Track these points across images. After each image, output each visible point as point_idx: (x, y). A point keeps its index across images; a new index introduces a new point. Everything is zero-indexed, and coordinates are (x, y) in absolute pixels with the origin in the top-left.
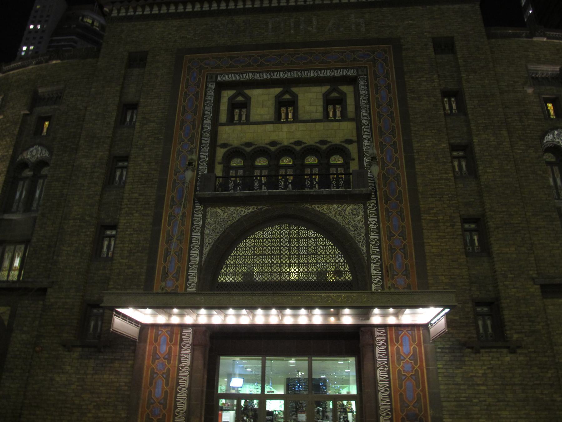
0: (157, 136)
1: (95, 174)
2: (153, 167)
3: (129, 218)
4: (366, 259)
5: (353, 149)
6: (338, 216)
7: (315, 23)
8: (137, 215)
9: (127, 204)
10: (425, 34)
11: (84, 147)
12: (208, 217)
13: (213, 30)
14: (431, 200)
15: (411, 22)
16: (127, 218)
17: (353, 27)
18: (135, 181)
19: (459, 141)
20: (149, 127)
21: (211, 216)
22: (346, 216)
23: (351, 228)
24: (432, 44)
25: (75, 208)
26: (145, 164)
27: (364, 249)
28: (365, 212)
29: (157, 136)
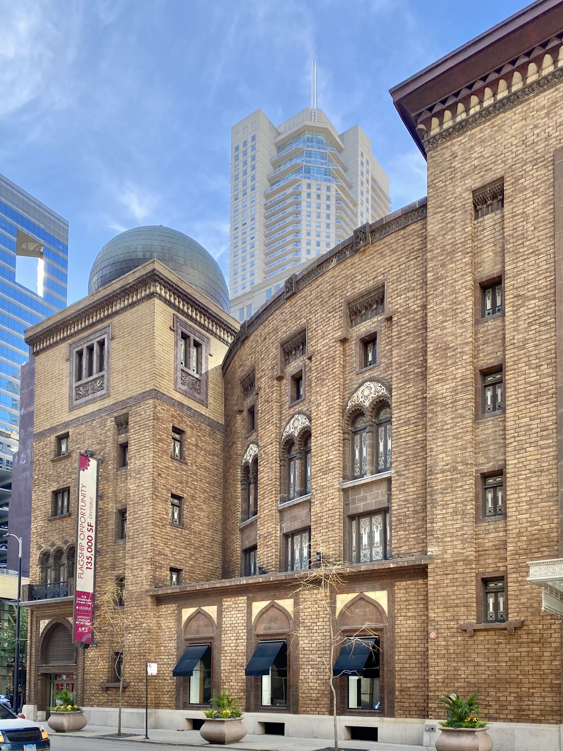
3: (521, 455)
9: (514, 437)
16: (517, 456)
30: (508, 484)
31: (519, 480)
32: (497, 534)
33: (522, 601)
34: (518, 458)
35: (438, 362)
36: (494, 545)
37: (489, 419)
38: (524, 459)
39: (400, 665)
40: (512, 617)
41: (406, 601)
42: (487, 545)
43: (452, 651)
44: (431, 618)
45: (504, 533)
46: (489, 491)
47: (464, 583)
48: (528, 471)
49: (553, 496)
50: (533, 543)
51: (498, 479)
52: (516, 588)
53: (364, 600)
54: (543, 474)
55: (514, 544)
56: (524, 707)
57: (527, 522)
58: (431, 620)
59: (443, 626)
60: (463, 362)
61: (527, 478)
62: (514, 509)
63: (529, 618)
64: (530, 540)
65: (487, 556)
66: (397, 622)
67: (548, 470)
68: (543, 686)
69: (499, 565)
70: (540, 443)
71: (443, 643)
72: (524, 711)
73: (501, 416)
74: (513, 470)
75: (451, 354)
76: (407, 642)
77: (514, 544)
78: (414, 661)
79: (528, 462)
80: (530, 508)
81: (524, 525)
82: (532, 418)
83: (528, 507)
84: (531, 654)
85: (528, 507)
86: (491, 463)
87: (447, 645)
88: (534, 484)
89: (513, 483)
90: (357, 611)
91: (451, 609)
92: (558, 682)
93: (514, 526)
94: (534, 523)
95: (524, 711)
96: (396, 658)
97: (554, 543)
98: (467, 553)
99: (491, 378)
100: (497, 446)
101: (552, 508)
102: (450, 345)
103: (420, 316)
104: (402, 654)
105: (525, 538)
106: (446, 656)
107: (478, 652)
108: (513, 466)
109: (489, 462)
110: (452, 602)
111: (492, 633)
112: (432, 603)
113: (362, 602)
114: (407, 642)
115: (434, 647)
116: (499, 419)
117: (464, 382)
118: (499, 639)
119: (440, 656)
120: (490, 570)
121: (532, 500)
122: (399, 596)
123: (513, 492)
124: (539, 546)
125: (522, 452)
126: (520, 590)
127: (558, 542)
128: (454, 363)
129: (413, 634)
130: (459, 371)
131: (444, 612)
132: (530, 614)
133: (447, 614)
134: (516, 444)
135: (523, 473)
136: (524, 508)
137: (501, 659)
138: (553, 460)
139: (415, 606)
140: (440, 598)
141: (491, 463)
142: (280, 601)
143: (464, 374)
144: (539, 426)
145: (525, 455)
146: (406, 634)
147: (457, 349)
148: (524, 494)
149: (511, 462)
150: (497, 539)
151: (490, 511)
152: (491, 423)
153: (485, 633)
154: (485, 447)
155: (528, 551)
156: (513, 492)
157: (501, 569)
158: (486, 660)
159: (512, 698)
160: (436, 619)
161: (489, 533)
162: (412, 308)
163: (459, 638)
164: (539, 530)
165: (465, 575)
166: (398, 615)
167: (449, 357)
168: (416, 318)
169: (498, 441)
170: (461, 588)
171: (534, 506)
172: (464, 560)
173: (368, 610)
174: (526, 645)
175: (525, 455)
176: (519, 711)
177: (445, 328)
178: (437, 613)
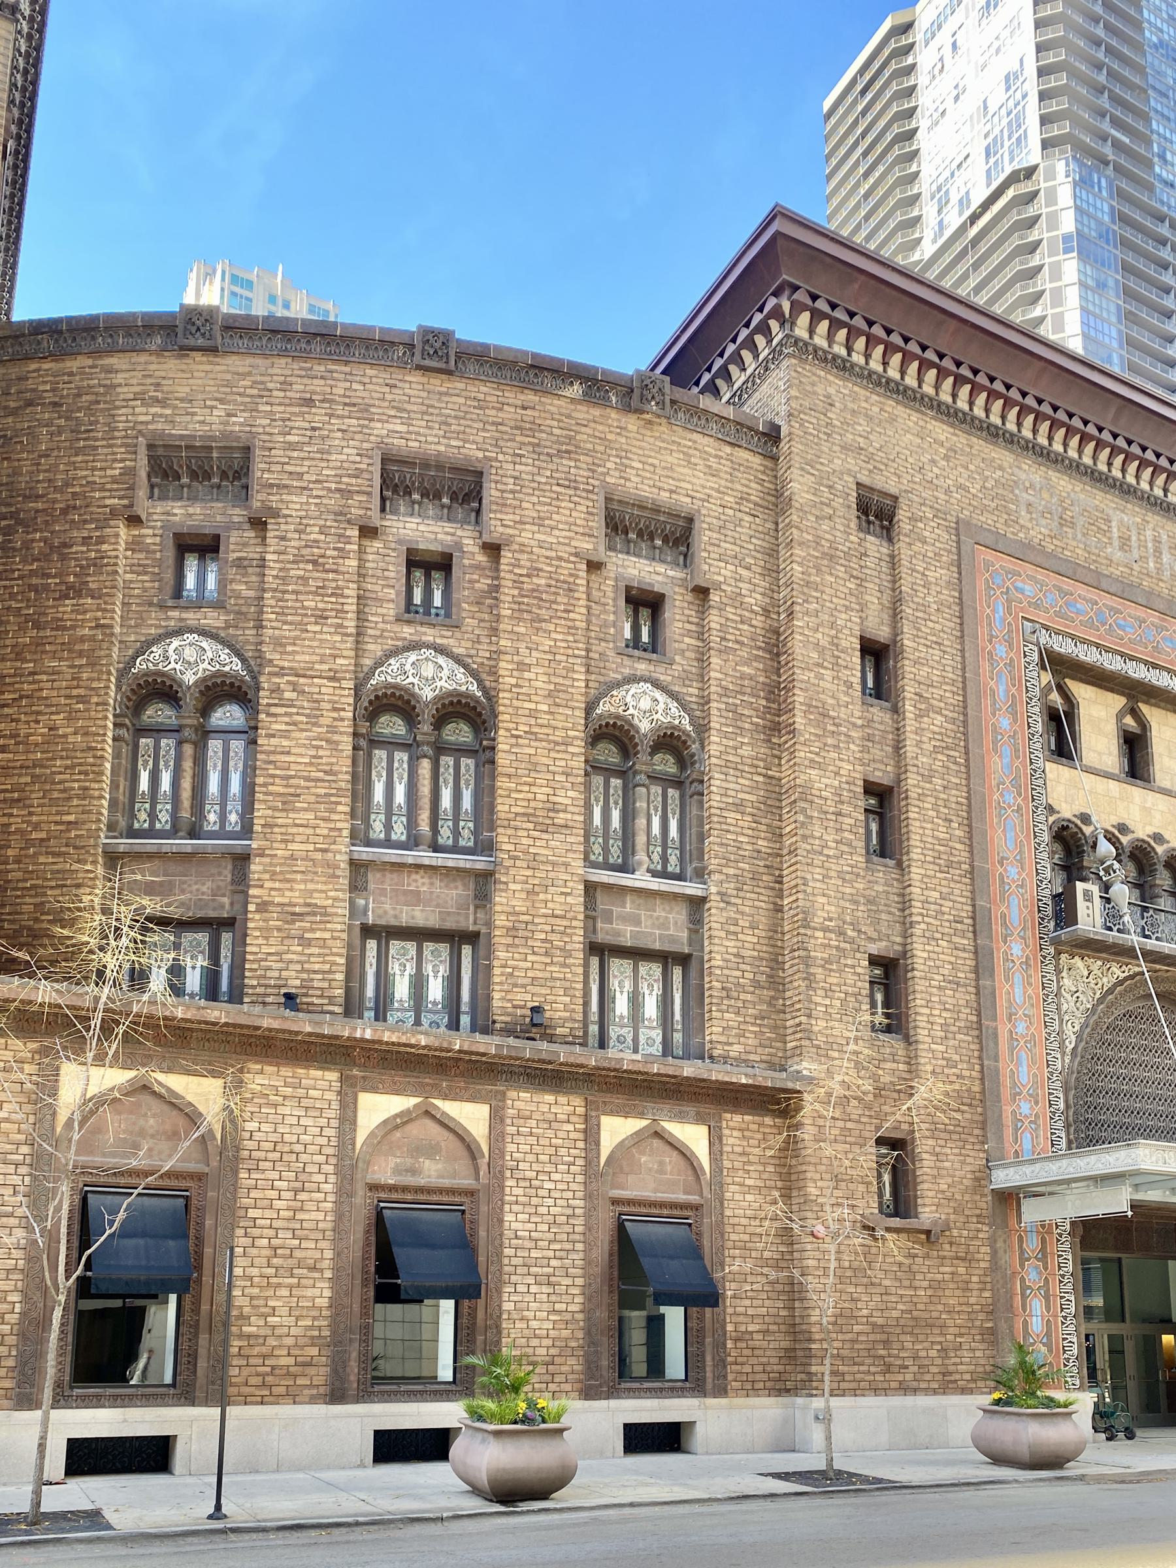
41: (744, 1154)
43: (847, 1264)
53: (662, 1138)
56: (951, 1368)
58: (812, 1201)
66: (728, 1195)
68: (973, 1331)
72: (951, 1373)
90: (643, 1159)
95: (951, 1373)
113: (656, 1143)
114: (746, 1238)
122: (731, 1141)
129: (757, 1222)
133: (837, 1193)
139: (761, 1168)
142: (447, 1103)
146: (744, 1221)
159: (933, 1353)
166: (729, 1180)
173: (667, 1160)
176: (944, 1374)
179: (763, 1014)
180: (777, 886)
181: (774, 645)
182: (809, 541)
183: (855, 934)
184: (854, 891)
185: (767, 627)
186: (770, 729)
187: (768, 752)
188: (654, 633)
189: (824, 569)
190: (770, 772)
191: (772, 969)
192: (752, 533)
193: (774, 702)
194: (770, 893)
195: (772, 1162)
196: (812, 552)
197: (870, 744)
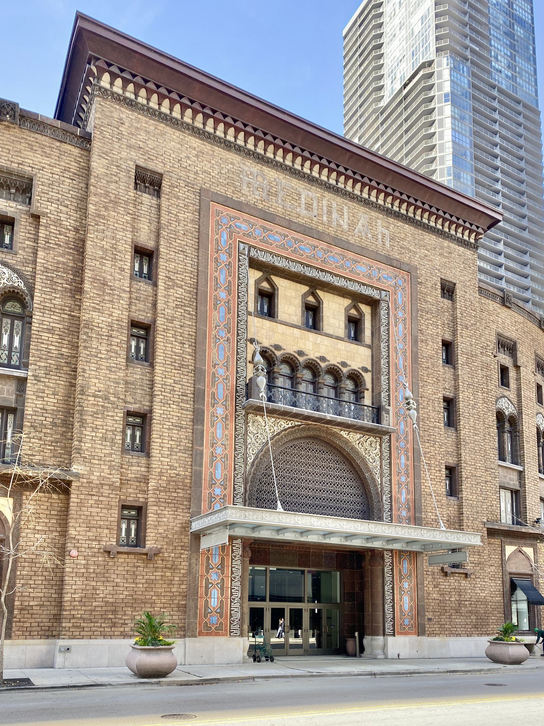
0: (187, 309)
1: (115, 340)
2: (187, 350)
4: (380, 489)
5: (367, 378)
6: (361, 446)
7: (346, 216)
8: (175, 407)
9: (161, 391)
10: (436, 271)
11: (92, 295)
12: (250, 424)
13: (241, 176)
14: (427, 444)
15: (426, 252)
16: (163, 408)
17: (380, 237)
18: (167, 362)
19: (448, 393)
20: (176, 293)
21: (253, 425)
22: (367, 447)
23: (370, 459)
24: (440, 285)
25: (93, 380)
26: (177, 343)
27: (379, 480)
28: (380, 445)
29: (187, 309)
30: (154, 428)
31: (163, 428)
32: (139, 468)
33: (160, 531)
34: (164, 410)
35: (96, 292)
36: (135, 477)
37: (138, 366)
38: (168, 413)
39: (22, 581)
40: (149, 544)
42: (129, 475)
43: (92, 571)
44: (72, 536)
45: (145, 470)
46: (129, 428)
47: (108, 507)
48: (171, 424)
49: (188, 451)
50: (171, 483)
51: (137, 420)
52: (155, 519)
54: (182, 430)
55: (156, 481)
57: (168, 465)
59: (83, 545)
60: (120, 305)
61: (169, 429)
62: (158, 451)
63: (165, 546)
64: (169, 481)
65: (129, 486)
66: (23, 534)
67: (186, 428)
69: (139, 495)
70: (181, 404)
71: (84, 562)
73: (148, 368)
74: (158, 418)
75: (109, 291)
76: (34, 557)
77: (156, 481)
78: (40, 578)
79: (171, 417)
80: (171, 455)
81: (165, 467)
82: (176, 382)
83: (169, 453)
84: (164, 578)
85: (169, 453)
86: (138, 405)
87: (87, 564)
88: (175, 435)
89: (158, 429)
91: (94, 530)
92: (184, 603)
93: (157, 466)
94: (172, 467)
96: (18, 573)
97: (187, 488)
98: (114, 480)
99: (135, 331)
100: (143, 392)
101: (187, 460)
102: (109, 283)
103: (72, 236)
104: (26, 569)
105: (165, 478)
106: (85, 575)
107: (118, 573)
108: (159, 415)
109: (135, 403)
110: (95, 522)
111: (132, 556)
112: (73, 521)
115: (72, 565)
116: (147, 370)
117: (120, 323)
118: (137, 563)
119: (78, 575)
120: (131, 499)
121: (173, 448)
123: (157, 436)
124: (176, 488)
125: (167, 406)
126: (158, 522)
127: (190, 487)
128: (110, 301)
130: (115, 311)
131: (86, 531)
132: (165, 543)
134: (162, 397)
135: (167, 423)
136: (166, 453)
137: (138, 581)
138: (190, 421)
139: (47, 521)
140: (82, 517)
141: (138, 405)
143: (120, 316)
144: (181, 391)
145: (169, 409)
147: (115, 290)
148: (167, 441)
149: (157, 411)
150: (139, 473)
151: (128, 446)
152: (139, 370)
153: (126, 556)
154: (133, 389)
155: (167, 490)
156: (157, 436)
157: (141, 500)
158: (125, 581)
160: (77, 537)
161: (132, 466)
162: (64, 223)
163: (100, 559)
164: (177, 475)
165: (110, 500)
167: (107, 293)
168: (68, 235)
169: (145, 388)
170: (105, 511)
171: (174, 453)
172: (110, 485)
174: (160, 570)
175: (169, 409)
177: (103, 264)
178: (79, 531)
179: (57, 440)
180: (73, 373)
181: (80, 247)
182: (102, 193)
183: (116, 399)
184: (117, 377)
185: (77, 238)
186: (74, 291)
187: (73, 303)
188: (11, 239)
189: (110, 208)
190: (72, 313)
191: (66, 417)
192: (71, 189)
193: (78, 277)
194: (68, 377)
195: (55, 517)
196: (103, 199)
197: (138, 302)
